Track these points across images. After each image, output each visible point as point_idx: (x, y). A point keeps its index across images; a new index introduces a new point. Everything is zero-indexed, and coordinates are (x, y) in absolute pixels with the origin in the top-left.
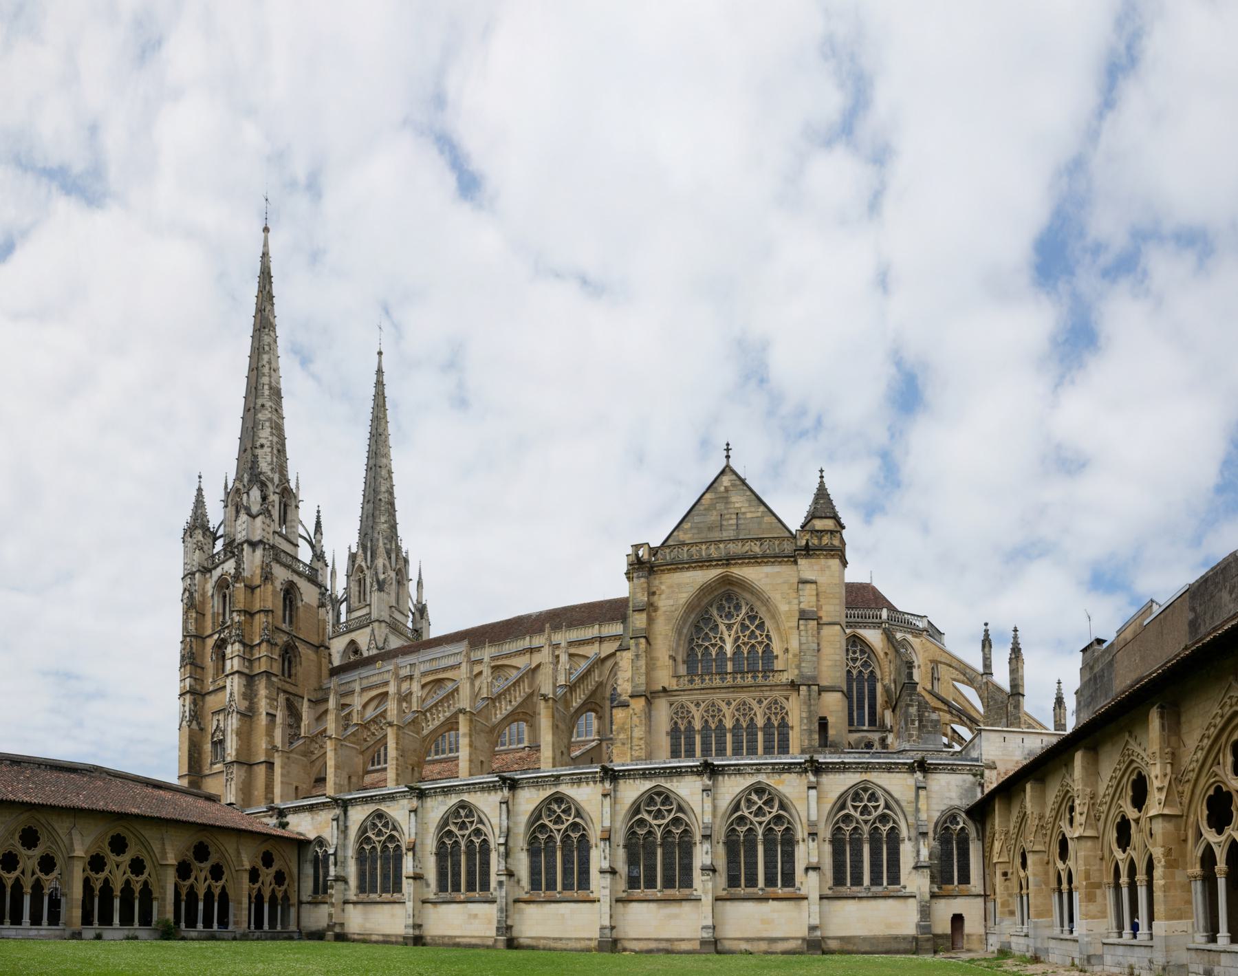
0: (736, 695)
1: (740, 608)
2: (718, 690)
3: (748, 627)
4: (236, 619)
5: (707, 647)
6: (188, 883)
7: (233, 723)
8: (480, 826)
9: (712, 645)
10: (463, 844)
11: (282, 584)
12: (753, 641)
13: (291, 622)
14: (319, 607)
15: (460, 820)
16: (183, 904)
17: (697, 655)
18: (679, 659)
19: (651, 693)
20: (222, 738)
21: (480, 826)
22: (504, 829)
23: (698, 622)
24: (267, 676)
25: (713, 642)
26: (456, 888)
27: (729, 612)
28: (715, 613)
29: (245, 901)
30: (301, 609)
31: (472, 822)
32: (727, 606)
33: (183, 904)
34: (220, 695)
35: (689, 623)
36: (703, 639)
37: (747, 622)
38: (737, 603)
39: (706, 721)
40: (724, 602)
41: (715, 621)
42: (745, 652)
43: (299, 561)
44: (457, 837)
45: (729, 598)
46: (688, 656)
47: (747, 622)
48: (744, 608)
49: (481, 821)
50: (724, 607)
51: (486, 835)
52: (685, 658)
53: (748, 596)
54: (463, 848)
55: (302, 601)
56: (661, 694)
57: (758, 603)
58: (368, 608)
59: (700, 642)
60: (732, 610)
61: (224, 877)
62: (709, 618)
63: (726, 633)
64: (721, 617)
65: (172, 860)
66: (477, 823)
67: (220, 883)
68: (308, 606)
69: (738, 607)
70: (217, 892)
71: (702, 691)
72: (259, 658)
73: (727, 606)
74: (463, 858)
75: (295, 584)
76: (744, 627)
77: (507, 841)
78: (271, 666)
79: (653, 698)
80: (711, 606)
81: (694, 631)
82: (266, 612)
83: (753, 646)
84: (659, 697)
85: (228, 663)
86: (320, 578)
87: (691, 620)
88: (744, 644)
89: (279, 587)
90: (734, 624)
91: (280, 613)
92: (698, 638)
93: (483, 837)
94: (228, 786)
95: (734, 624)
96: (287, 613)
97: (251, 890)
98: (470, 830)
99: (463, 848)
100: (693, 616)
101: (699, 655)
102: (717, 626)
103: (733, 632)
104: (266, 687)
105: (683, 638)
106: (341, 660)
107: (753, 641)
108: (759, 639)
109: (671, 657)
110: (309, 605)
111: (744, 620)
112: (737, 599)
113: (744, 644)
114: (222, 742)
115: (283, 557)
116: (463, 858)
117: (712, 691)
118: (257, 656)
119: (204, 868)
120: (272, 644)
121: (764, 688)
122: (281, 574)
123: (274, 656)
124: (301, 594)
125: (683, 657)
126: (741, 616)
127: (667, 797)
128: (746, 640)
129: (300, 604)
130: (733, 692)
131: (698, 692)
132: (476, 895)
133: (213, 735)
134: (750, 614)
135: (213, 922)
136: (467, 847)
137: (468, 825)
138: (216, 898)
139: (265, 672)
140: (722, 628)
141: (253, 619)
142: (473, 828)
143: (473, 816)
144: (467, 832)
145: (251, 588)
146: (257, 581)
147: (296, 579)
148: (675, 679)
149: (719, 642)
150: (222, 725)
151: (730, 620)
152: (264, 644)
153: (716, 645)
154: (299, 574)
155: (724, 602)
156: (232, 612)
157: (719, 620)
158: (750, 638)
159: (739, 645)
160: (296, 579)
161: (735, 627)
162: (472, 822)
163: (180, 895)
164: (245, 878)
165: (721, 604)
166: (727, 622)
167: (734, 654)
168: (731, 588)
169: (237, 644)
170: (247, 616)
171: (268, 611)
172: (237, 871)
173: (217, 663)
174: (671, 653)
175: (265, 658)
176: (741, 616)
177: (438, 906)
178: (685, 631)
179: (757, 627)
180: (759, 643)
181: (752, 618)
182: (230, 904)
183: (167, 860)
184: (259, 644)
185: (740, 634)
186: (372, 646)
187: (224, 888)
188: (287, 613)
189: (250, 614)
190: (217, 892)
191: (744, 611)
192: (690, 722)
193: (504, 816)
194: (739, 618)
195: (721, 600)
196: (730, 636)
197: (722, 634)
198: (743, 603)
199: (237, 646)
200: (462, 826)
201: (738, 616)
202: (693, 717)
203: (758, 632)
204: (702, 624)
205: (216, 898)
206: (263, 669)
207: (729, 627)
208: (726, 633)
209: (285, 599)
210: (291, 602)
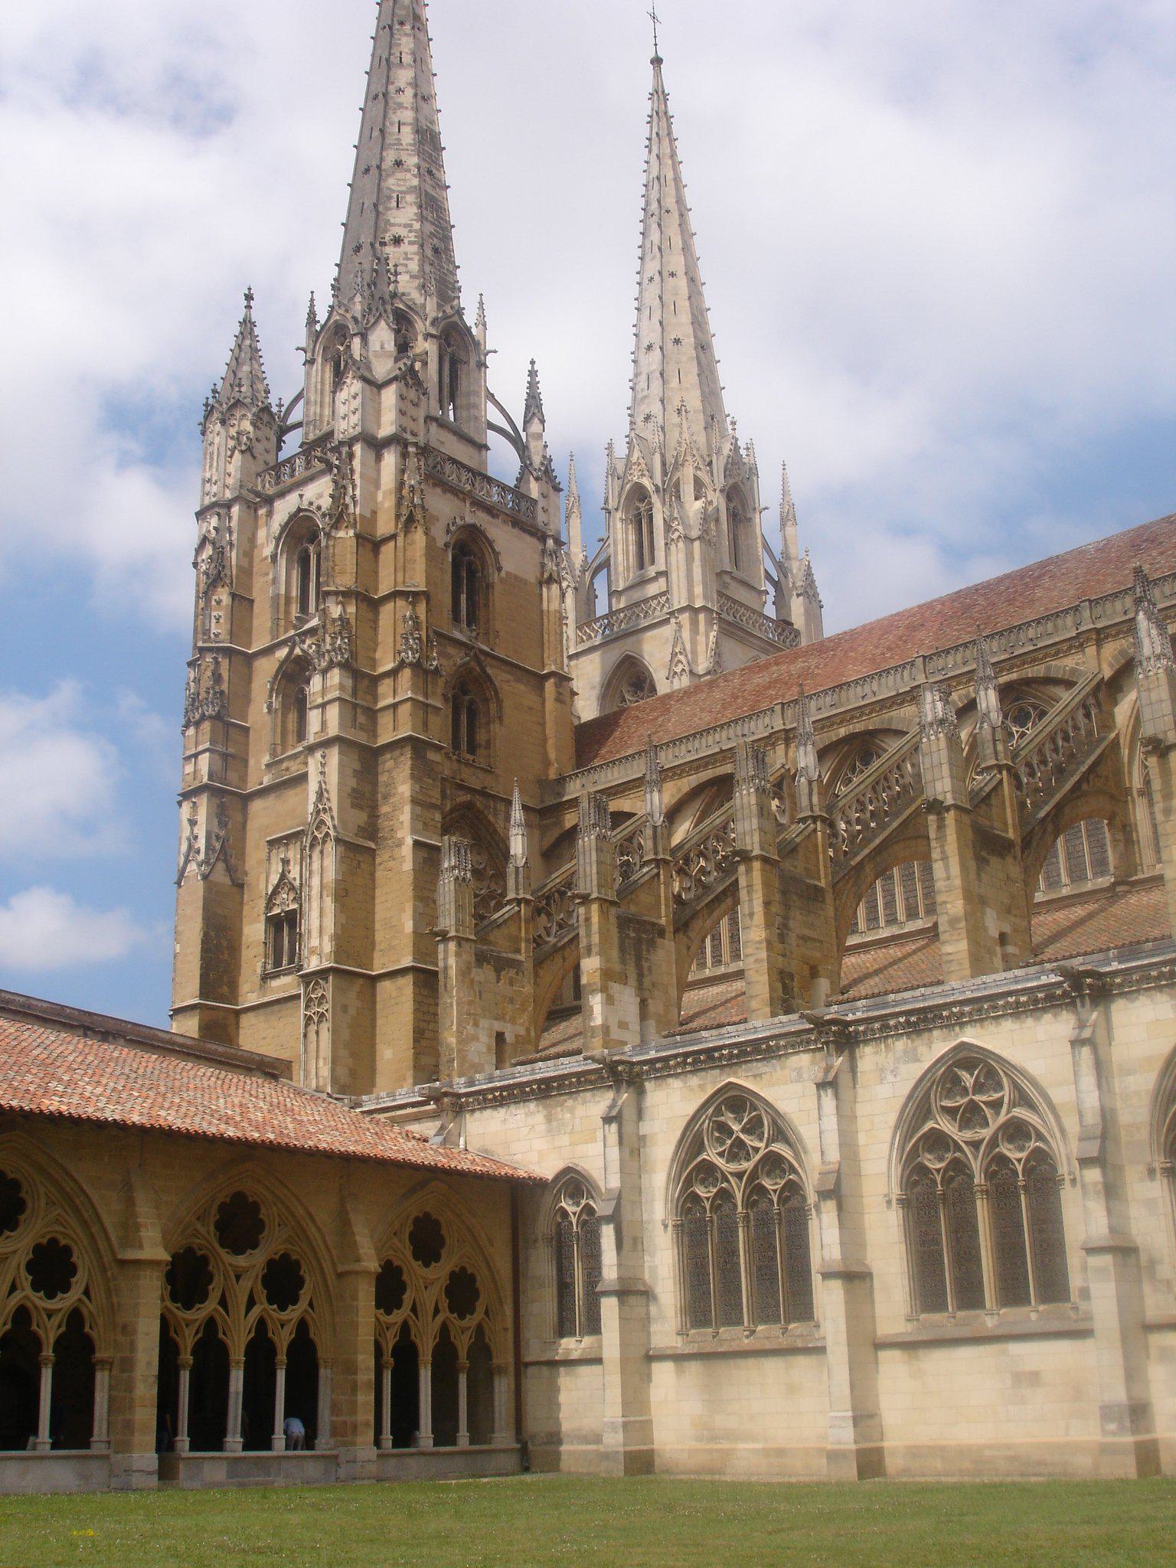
4: (335, 611)
6: (199, 1314)
7: (326, 865)
8: (1021, 1112)
10: (976, 1166)
11: (448, 531)
13: (472, 620)
14: (541, 584)
15: (962, 1101)
16: (185, 1377)
20: (295, 906)
21: (1021, 1112)
22: (1092, 1118)
24: (415, 750)
26: (970, 1297)
29: (366, 1360)
30: (498, 589)
31: (996, 1105)
33: (185, 1377)
34: (291, 796)
43: (490, 480)
44: (958, 1148)
49: (1023, 1099)
51: (1040, 1137)
54: (979, 1179)
55: (499, 569)
58: (662, 581)
61: (305, 1295)
65: (153, 1248)
66: (1013, 1104)
67: (294, 1313)
68: (515, 581)
70: (283, 1339)
72: (395, 706)
74: (982, 1212)
75: (482, 533)
77: (1103, 1148)
78: (425, 724)
82: (413, 597)
85: (314, 718)
86: (541, 517)
89: (442, 539)
91: (447, 599)
93: (1033, 1144)
94: (312, 1036)
96: (463, 597)
97: (380, 1329)
98: (994, 1125)
99: (979, 1179)
104: (413, 776)
106: (602, 706)
110: (516, 578)
114: (291, 920)
115: (451, 474)
116: (982, 1212)
118: (390, 701)
119: (246, 1270)
120: (426, 672)
122: (444, 508)
123: (430, 701)
124: (496, 554)
129: (495, 578)
132: (1033, 1314)
133: (270, 900)
135: (271, 1430)
136: (990, 1176)
137: (988, 1112)
138: (282, 1357)
139: (410, 738)
141: (377, 613)
142: (1003, 1118)
143: (999, 1086)
144: (986, 1133)
145: (370, 544)
146: (385, 525)
147: (481, 519)
150: (294, 873)
152: (406, 674)
154: (490, 510)
156: (322, 596)
160: (481, 519)
162: (996, 1105)
163: (177, 1352)
164: (365, 1295)
169: (336, 671)
170: (364, 606)
171: (415, 594)
172: (340, 1276)
173: (284, 716)
175: (408, 705)
177: (921, 1353)
182: (322, 1372)
183: (141, 1247)
184: (393, 673)
186: (678, 669)
187: (302, 1326)
188: (463, 597)
189: (370, 603)
190: (283, 1339)
193: (1088, 1080)
199: (335, 676)
200: (971, 1116)
205: (282, 1357)
206: (405, 732)
209: (456, 566)
210: (472, 573)
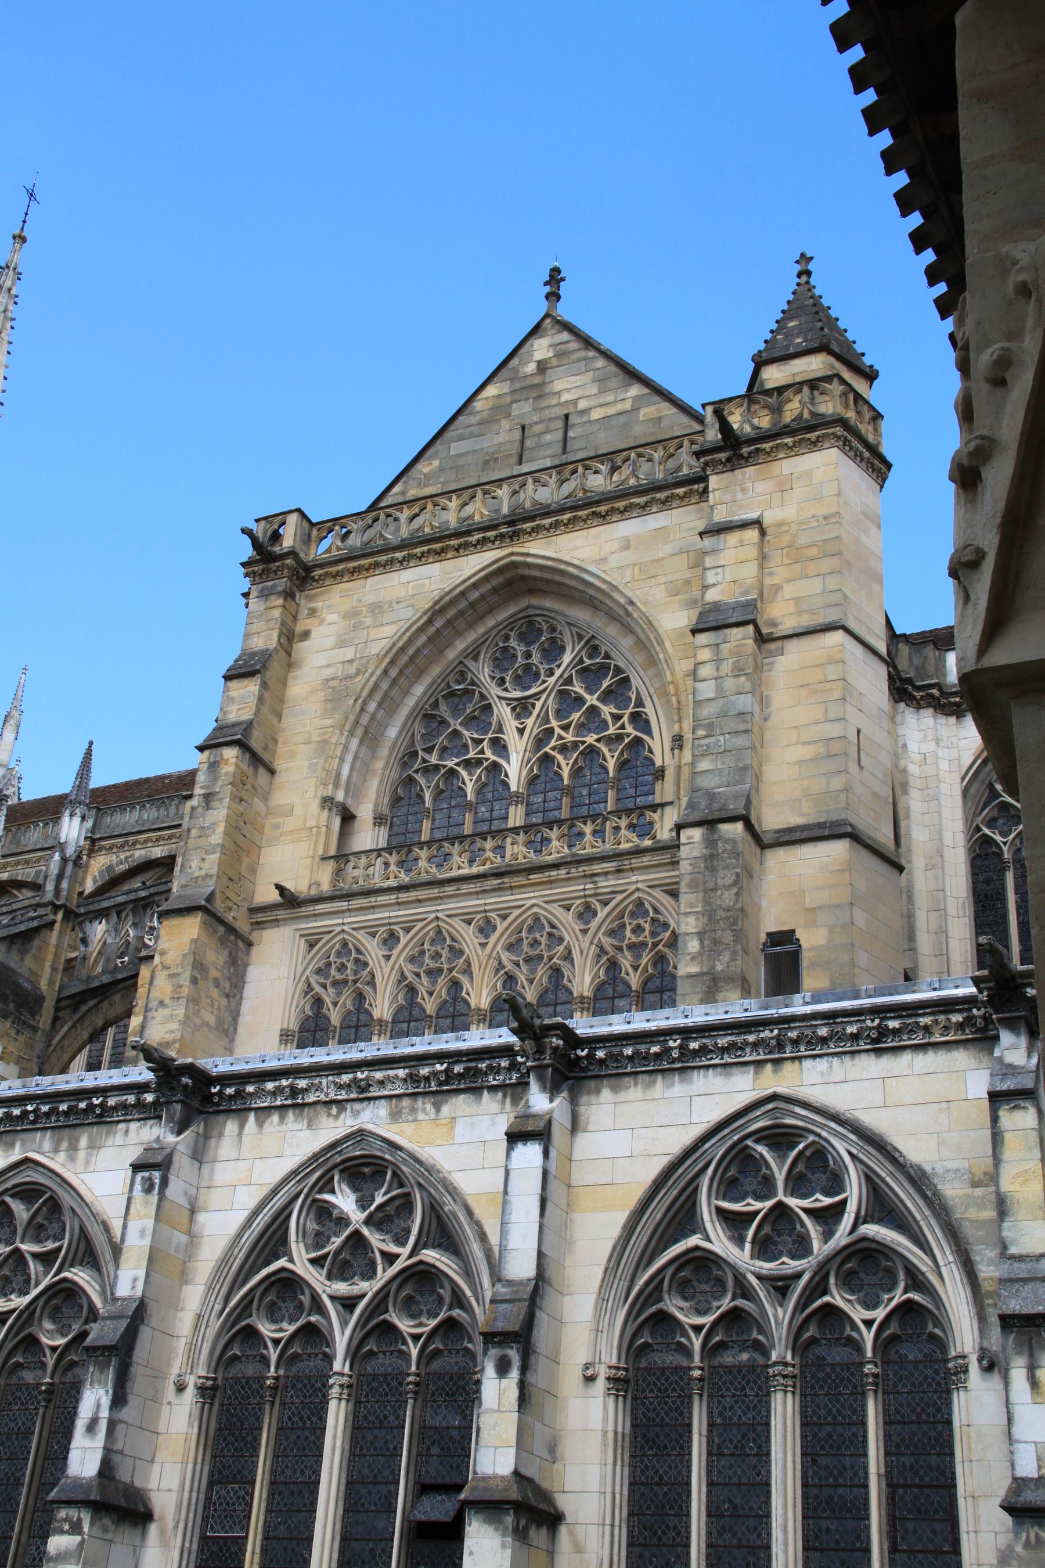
0: (506, 899)
1: (562, 649)
2: (450, 890)
3: (580, 700)
5: (452, 773)
9: (468, 764)
12: (591, 739)
17: (420, 797)
18: (365, 812)
19: (253, 911)
23: (435, 705)
25: (471, 754)
27: (527, 668)
28: (483, 672)
32: (520, 649)
35: (404, 712)
36: (444, 750)
37: (578, 688)
38: (553, 640)
39: (412, 990)
40: (513, 643)
41: (483, 697)
42: (566, 772)
45: (529, 630)
46: (396, 801)
47: (578, 688)
48: (569, 649)
50: (515, 656)
52: (386, 811)
53: (581, 615)
56: (281, 914)
57: (612, 630)
59: (434, 759)
60: (536, 659)
62: (466, 691)
63: (511, 724)
64: (501, 682)
69: (553, 650)
71: (404, 896)
73: (520, 649)
76: (568, 701)
79: (259, 925)
80: (476, 658)
81: (419, 728)
83: (592, 751)
84: (276, 922)
87: (411, 702)
88: (563, 749)
90: (537, 696)
92: (429, 750)
95: (537, 696)
100: (419, 690)
101: (428, 796)
102: (488, 708)
103: (530, 722)
105: (384, 752)
107: (591, 739)
108: (612, 730)
109: (327, 802)
111: (569, 681)
112: (553, 629)
113: (563, 749)
117: (435, 892)
121: (597, 868)
125: (376, 805)
126: (558, 673)
127: (54, 1206)
128: (570, 737)
130: (498, 889)
131: (391, 898)
134: (588, 662)
140: (503, 712)
148: (330, 866)
149: (488, 754)
151: (529, 687)
153: (479, 762)
155: (513, 643)
157: (495, 691)
158: (582, 728)
159: (546, 754)
161: (538, 705)
165: (505, 649)
166: (518, 694)
167: (532, 781)
168: (535, 601)
174: (329, 791)
176: (558, 673)
178: (392, 732)
179: (605, 697)
180: (610, 740)
181: (590, 675)
185: (554, 723)
191: (567, 658)
192: (360, 997)
194: (552, 680)
195: (507, 638)
196: (521, 731)
197: (500, 729)
198: (567, 638)
201: (551, 673)
202: (372, 982)
203: (607, 710)
204: (444, 710)
207: (522, 707)
208: (511, 724)
